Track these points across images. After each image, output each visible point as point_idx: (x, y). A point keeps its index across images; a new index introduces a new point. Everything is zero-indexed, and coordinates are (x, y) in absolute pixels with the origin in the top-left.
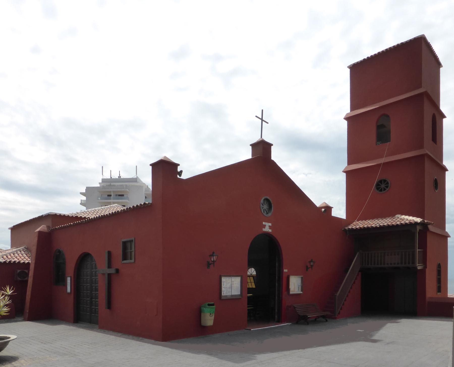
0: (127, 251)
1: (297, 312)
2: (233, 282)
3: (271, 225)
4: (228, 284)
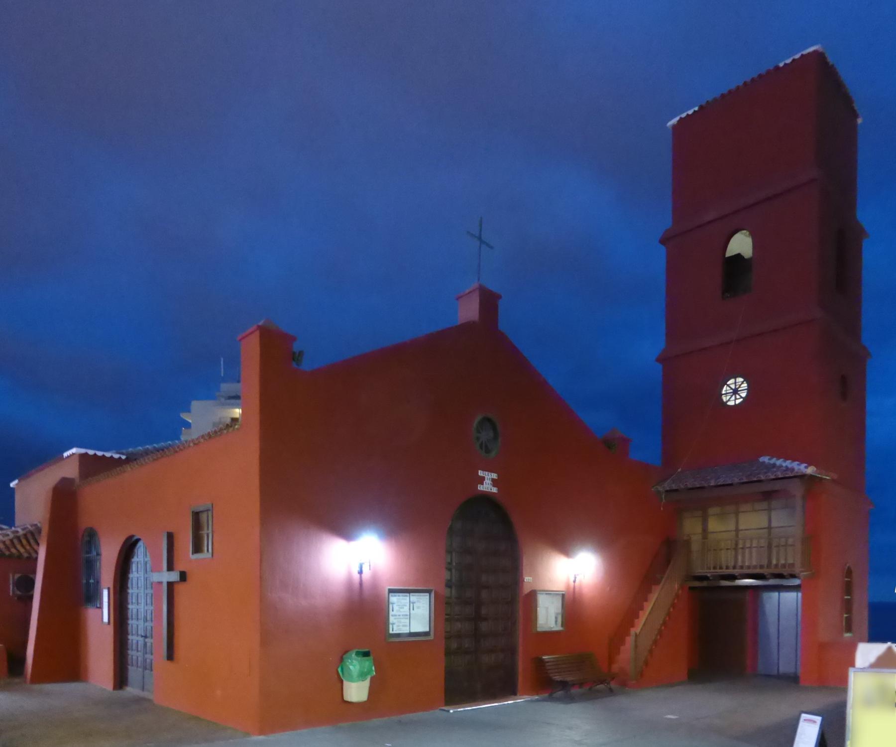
0: (203, 532)
1: (550, 671)
2: (413, 603)
3: (497, 478)
4: (403, 608)
